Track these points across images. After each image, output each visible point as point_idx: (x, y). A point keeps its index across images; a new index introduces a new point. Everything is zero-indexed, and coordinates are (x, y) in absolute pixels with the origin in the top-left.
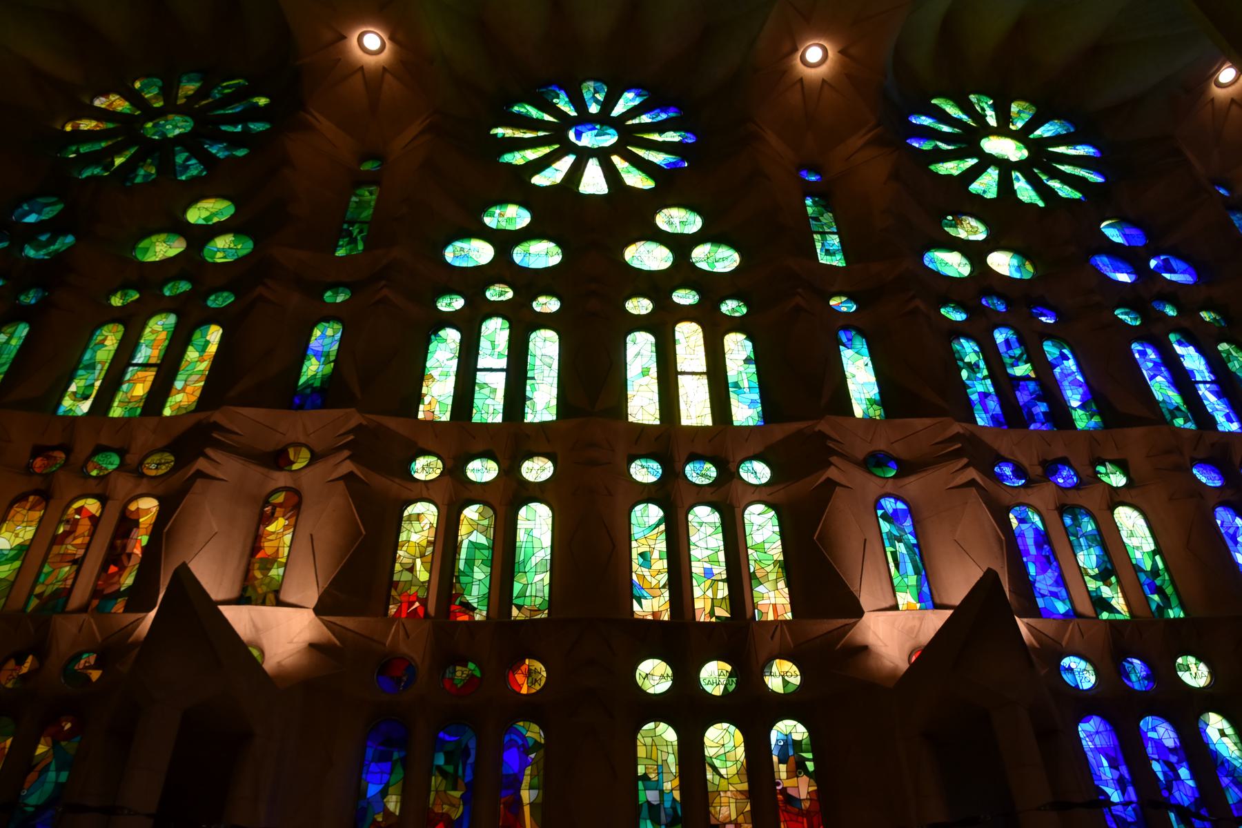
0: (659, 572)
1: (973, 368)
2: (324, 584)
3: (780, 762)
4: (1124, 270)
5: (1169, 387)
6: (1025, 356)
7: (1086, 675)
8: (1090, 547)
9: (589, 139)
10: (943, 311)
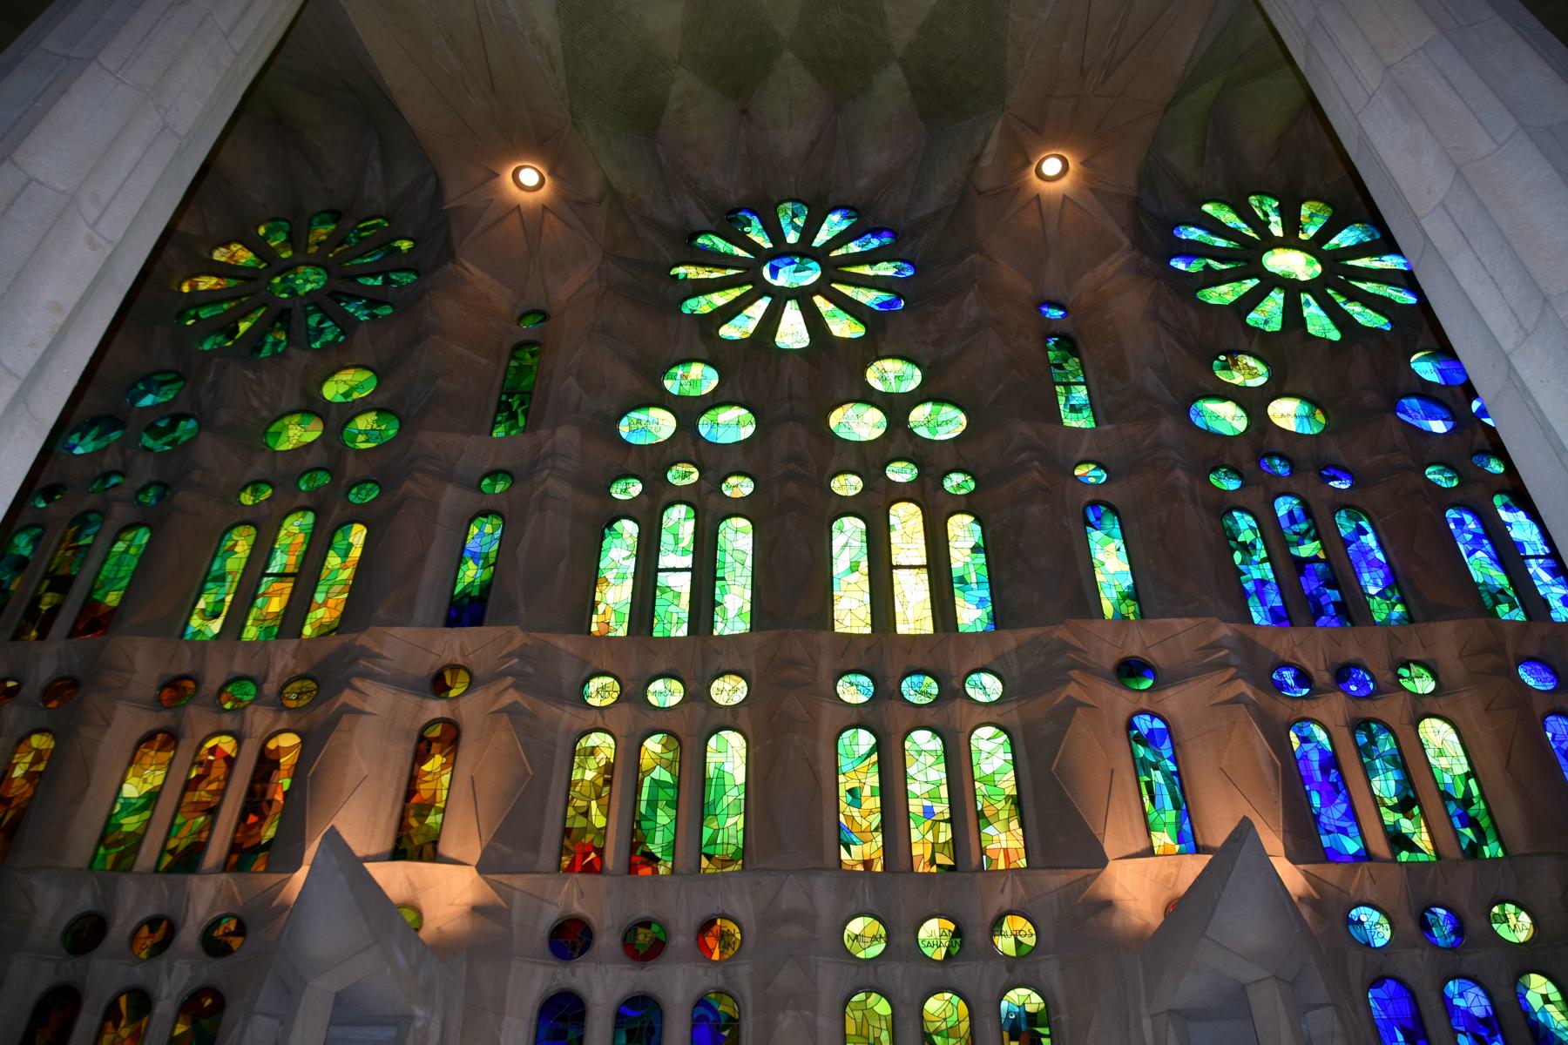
0: (871, 812)
1: (1247, 548)
2: (487, 837)
4: (1438, 416)
5: (1492, 564)
6: (1312, 533)
7: (1379, 930)
8: (1387, 770)
9: (786, 278)
10: (1213, 478)
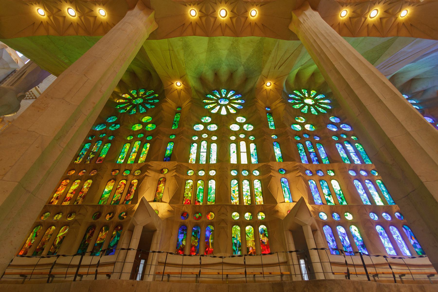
0: (237, 194)
1: (301, 150)
3: (261, 234)
